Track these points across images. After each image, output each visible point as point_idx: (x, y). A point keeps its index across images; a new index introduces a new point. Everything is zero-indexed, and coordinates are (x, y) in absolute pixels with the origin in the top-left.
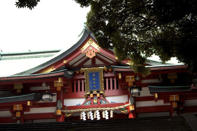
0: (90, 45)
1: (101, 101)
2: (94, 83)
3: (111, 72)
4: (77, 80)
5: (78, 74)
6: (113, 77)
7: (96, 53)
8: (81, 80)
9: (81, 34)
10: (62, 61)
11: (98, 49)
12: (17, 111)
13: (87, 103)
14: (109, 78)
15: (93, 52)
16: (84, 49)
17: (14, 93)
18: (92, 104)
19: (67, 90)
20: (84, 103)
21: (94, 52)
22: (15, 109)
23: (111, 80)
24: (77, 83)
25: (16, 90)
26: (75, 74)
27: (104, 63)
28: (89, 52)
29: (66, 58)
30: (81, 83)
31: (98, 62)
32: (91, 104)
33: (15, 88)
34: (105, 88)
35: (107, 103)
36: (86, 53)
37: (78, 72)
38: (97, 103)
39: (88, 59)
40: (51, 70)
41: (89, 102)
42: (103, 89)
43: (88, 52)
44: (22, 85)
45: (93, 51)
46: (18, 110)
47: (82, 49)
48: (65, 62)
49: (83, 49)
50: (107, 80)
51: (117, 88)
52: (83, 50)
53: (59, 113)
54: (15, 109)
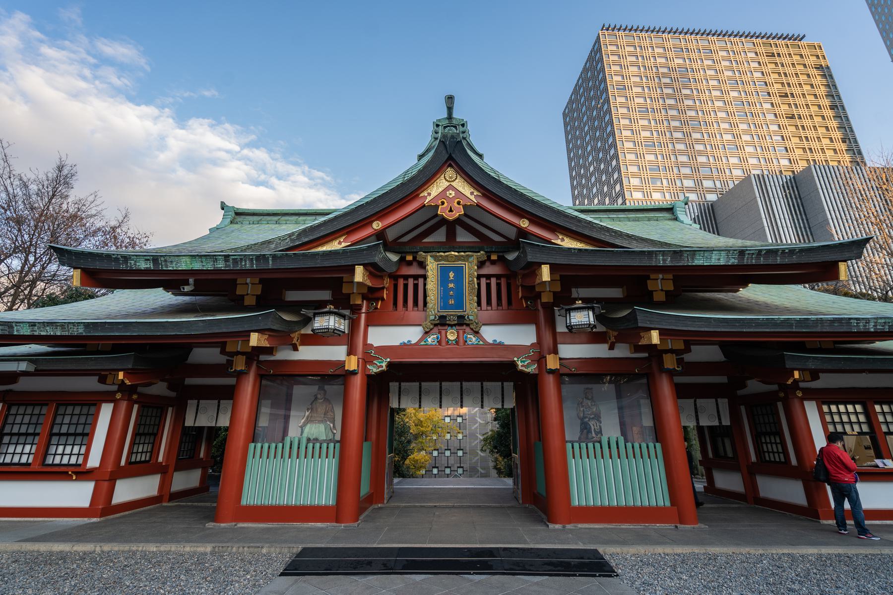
0: (447, 184)
1: (467, 337)
2: (451, 285)
3: (493, 263)
4: (406, 277)
5: (409, 263)
6: (498, 277)
7: (465, 206)
8: (416, 277)
9: (428, 151)
10: (366, 222)
11: (472, 198)
12: (238, 353)
13: (429, 340)
14: (488, 277)
15: (455, 204)
16: (432, 197)
17: (238, 305)
18: (443, 343)
19: (377, 304)
20: (420, 340)
21: (459, 203)
22: (229, 349)
23: (493, 281)
24: (406, 286)
25: (242, 296)
26: (402, 260)
27: (478, 240)
28: (446, 204)
29: (381, 215)
30: (416, 286)
31: (463, 237)
32: (439, 342)
33: (239, 291)
34: (479, 303)
35: (481, 343)
36: (437, 207)
37: (409, 258)
38: (457, 343)
39: (443, 221)
40: (335, 246)
41: (435, 336)
42: (476, 304)
43: (443, 203)
44: (261, 286)
45: (456, 201)
46: (239, 350)
47: (425, 194)
48: (377, 225)
49: (429, 194)
50: (483, 281)
51: (510, 302)
52: (429, 199)
53: (352, 364)
54: (229, 349)
